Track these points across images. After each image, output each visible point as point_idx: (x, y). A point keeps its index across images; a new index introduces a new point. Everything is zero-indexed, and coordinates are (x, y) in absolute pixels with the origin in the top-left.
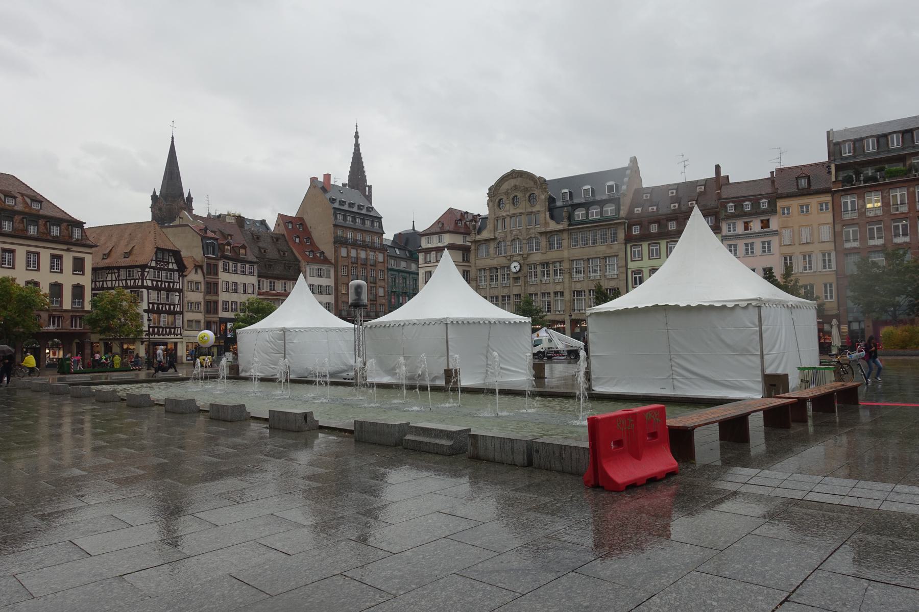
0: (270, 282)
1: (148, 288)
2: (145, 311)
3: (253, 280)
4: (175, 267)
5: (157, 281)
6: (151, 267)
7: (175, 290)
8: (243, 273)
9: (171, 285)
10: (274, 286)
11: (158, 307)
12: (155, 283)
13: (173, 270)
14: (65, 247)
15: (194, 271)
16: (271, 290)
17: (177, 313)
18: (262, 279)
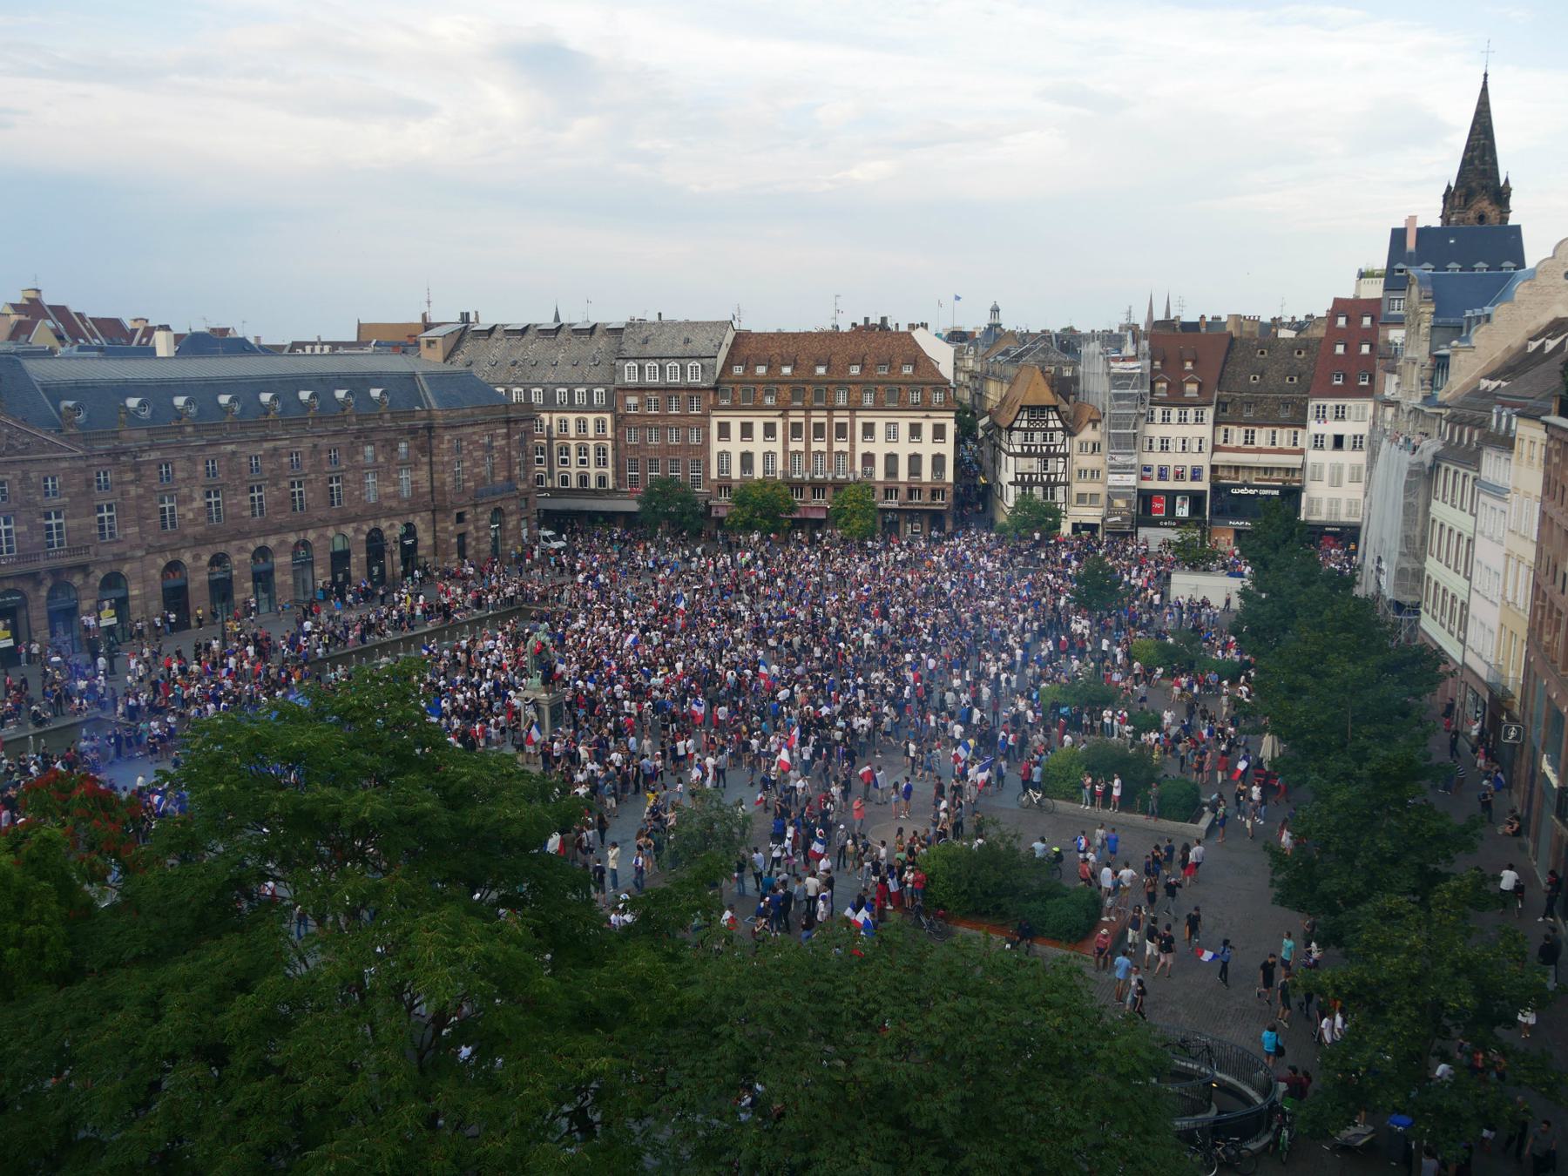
0: (1247, 432)
1: (1015, 455)
2: (1011, 483)
3: (1205, 431)
4: (1059, 424)
5: (1029, 446)
6: (1019, 429)
7: (1060, 455)
8: (1182, 421)
9: (1052, 448)
10: (1253, 437)
11: (1030, 478)
12: (1026, 448)
13: (1056, 429)
14: (924, 414)
15: (1090, 425)
16: (1246, 443)
17: (1061, 484)
18: (1230, 427)
